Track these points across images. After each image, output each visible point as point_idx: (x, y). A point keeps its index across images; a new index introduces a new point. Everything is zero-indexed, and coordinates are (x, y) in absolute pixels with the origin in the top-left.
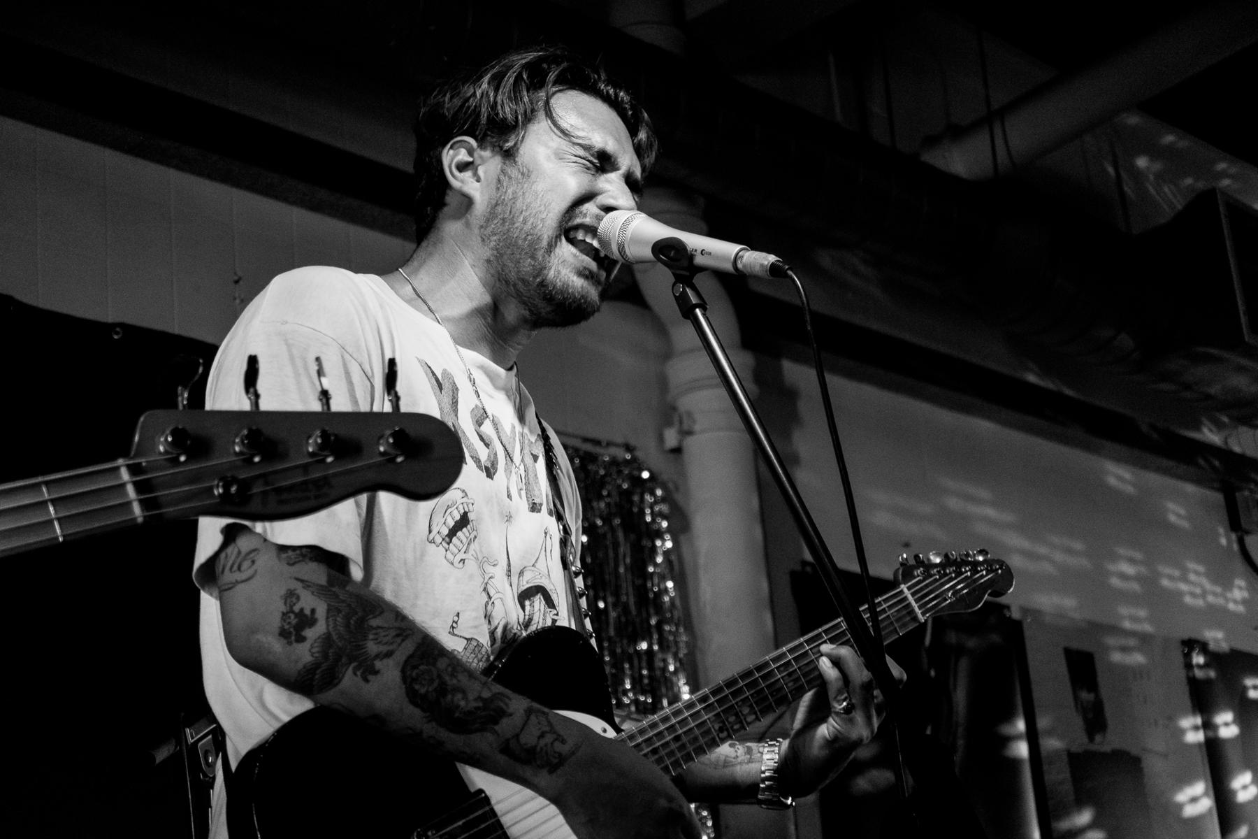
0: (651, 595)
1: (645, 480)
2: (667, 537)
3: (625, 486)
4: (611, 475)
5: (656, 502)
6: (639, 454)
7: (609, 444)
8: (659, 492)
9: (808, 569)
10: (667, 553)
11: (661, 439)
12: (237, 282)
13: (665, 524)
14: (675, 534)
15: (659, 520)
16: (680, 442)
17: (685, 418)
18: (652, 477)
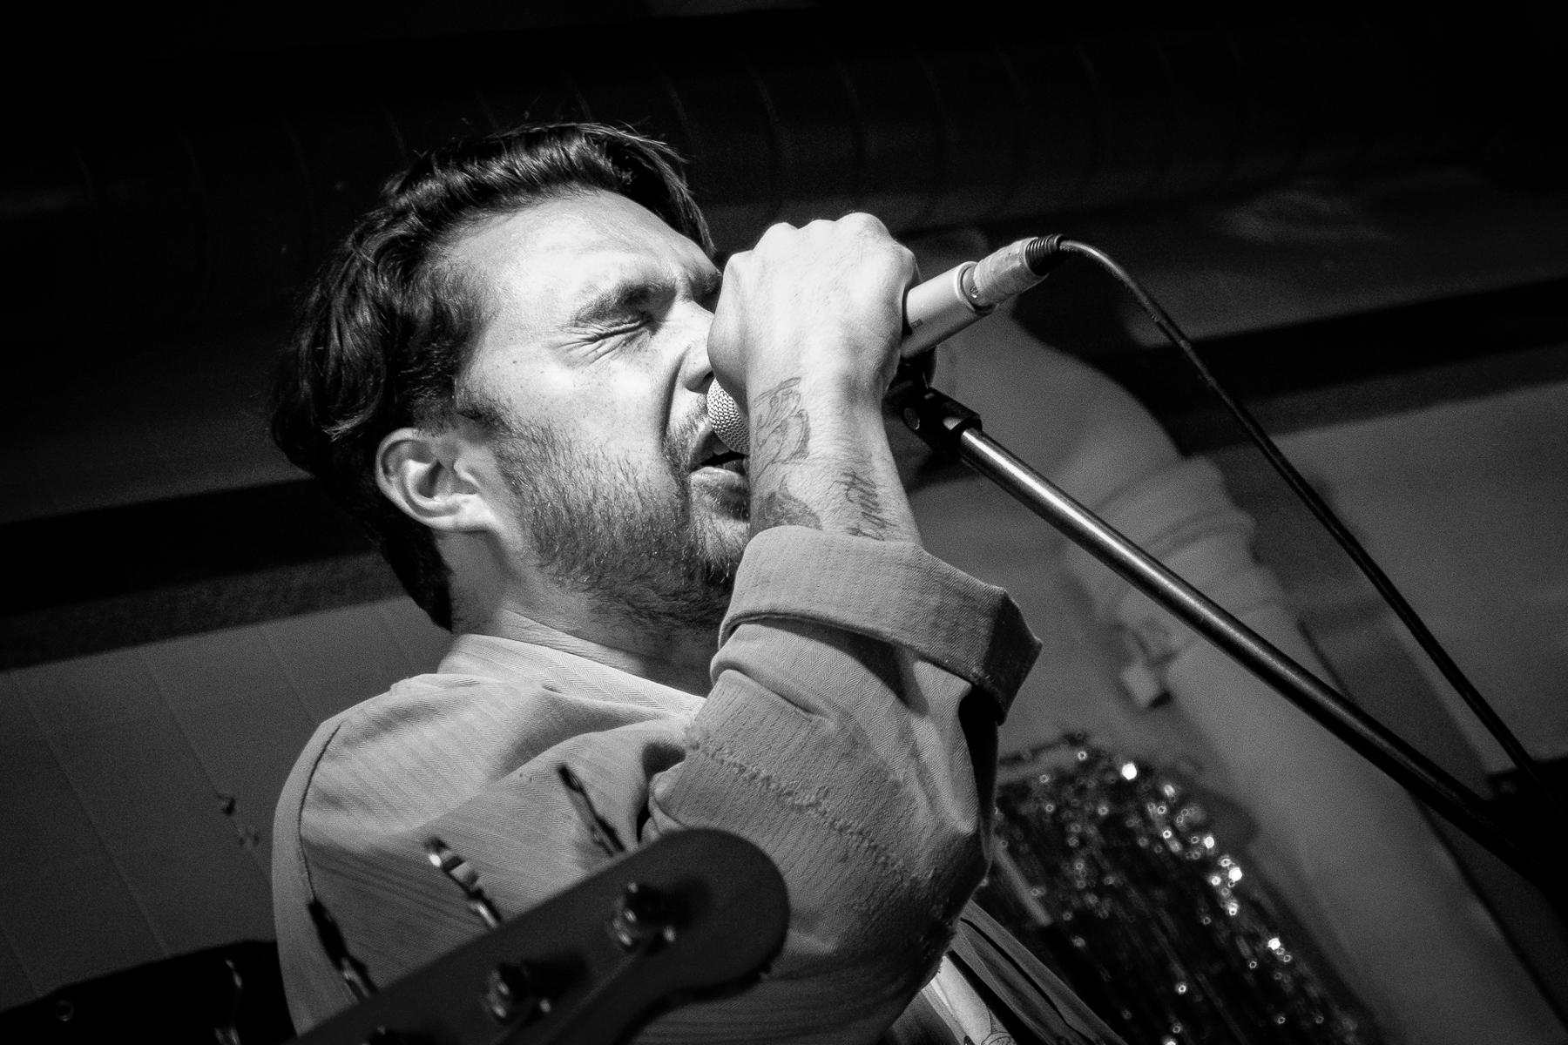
0: (1249, 978)
1: (1134, 782)
2: (1226, 862)
3: (1103, 810)
4: (1068, 805)
5: (1174, 809)
6: (1097, 741)
7: (1036, 752)
8: (1169, 790)
9: (1507, 787)
10: (1239, 891)
11: (1125, 694)
12: (230, 810)
13: (1209, 842)
14: (1237, 848)
15: (1194, 839)
16: (1161, 682)
17: (1145, 634)
18: (1144, 770)
